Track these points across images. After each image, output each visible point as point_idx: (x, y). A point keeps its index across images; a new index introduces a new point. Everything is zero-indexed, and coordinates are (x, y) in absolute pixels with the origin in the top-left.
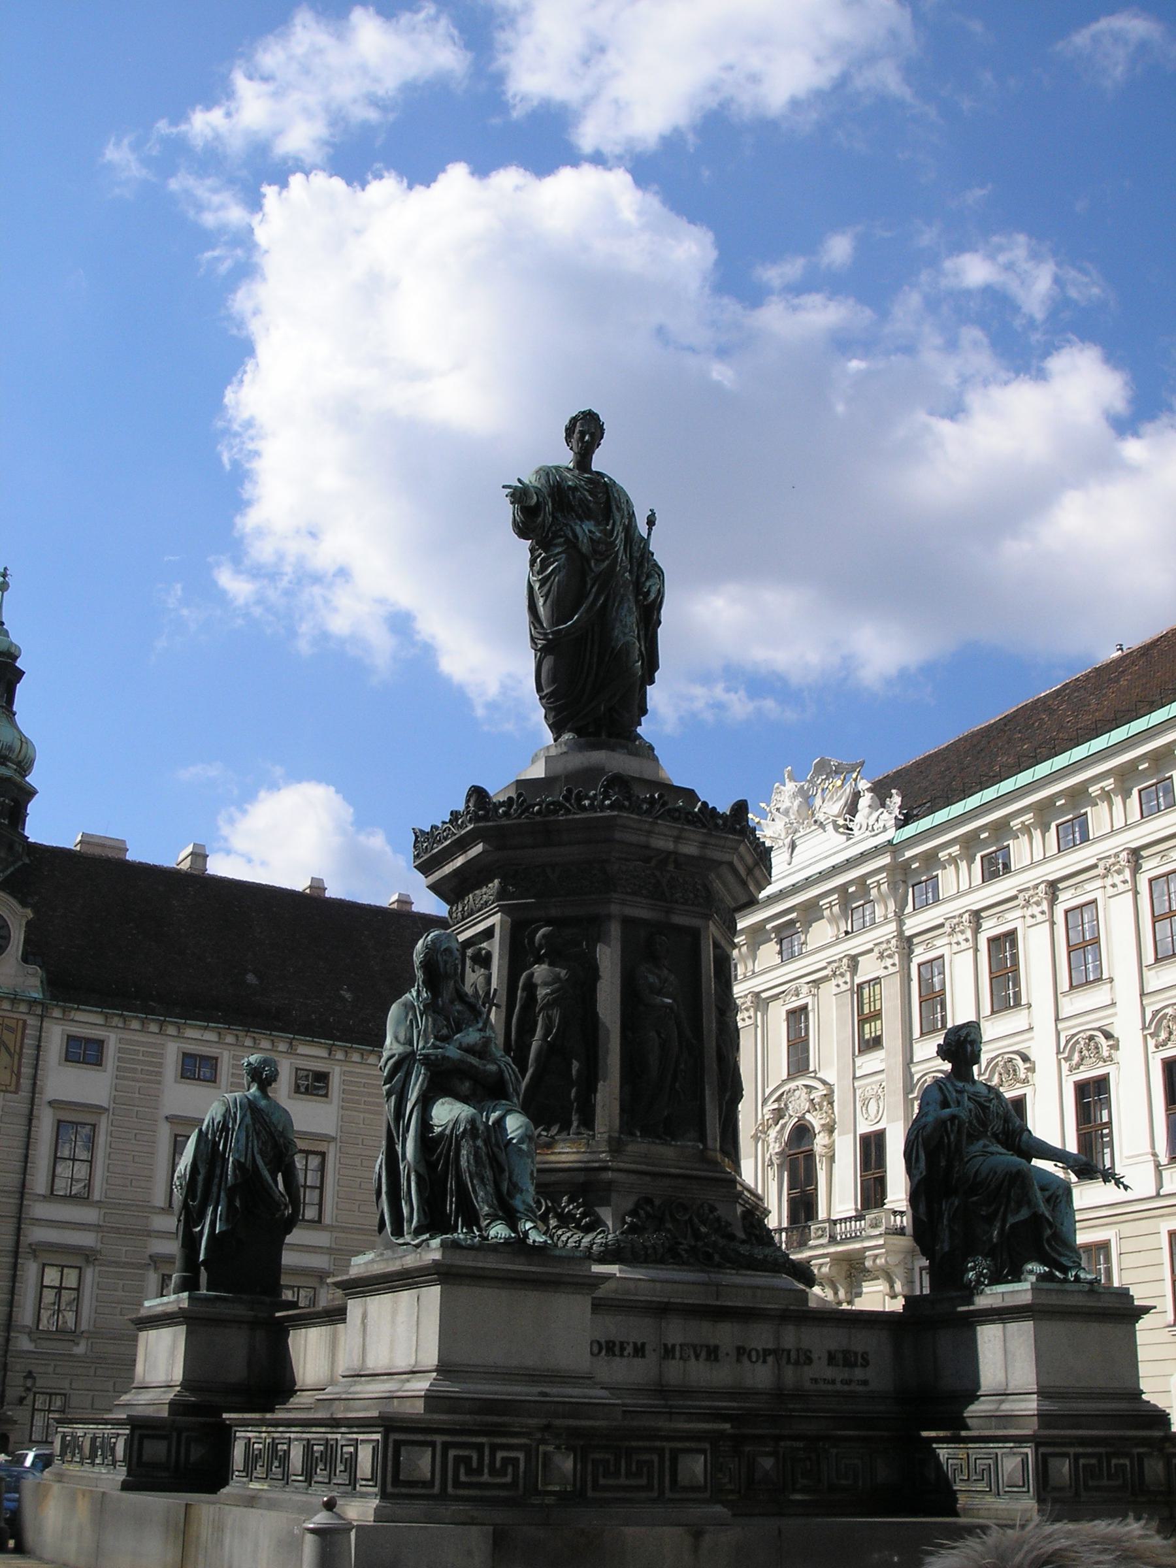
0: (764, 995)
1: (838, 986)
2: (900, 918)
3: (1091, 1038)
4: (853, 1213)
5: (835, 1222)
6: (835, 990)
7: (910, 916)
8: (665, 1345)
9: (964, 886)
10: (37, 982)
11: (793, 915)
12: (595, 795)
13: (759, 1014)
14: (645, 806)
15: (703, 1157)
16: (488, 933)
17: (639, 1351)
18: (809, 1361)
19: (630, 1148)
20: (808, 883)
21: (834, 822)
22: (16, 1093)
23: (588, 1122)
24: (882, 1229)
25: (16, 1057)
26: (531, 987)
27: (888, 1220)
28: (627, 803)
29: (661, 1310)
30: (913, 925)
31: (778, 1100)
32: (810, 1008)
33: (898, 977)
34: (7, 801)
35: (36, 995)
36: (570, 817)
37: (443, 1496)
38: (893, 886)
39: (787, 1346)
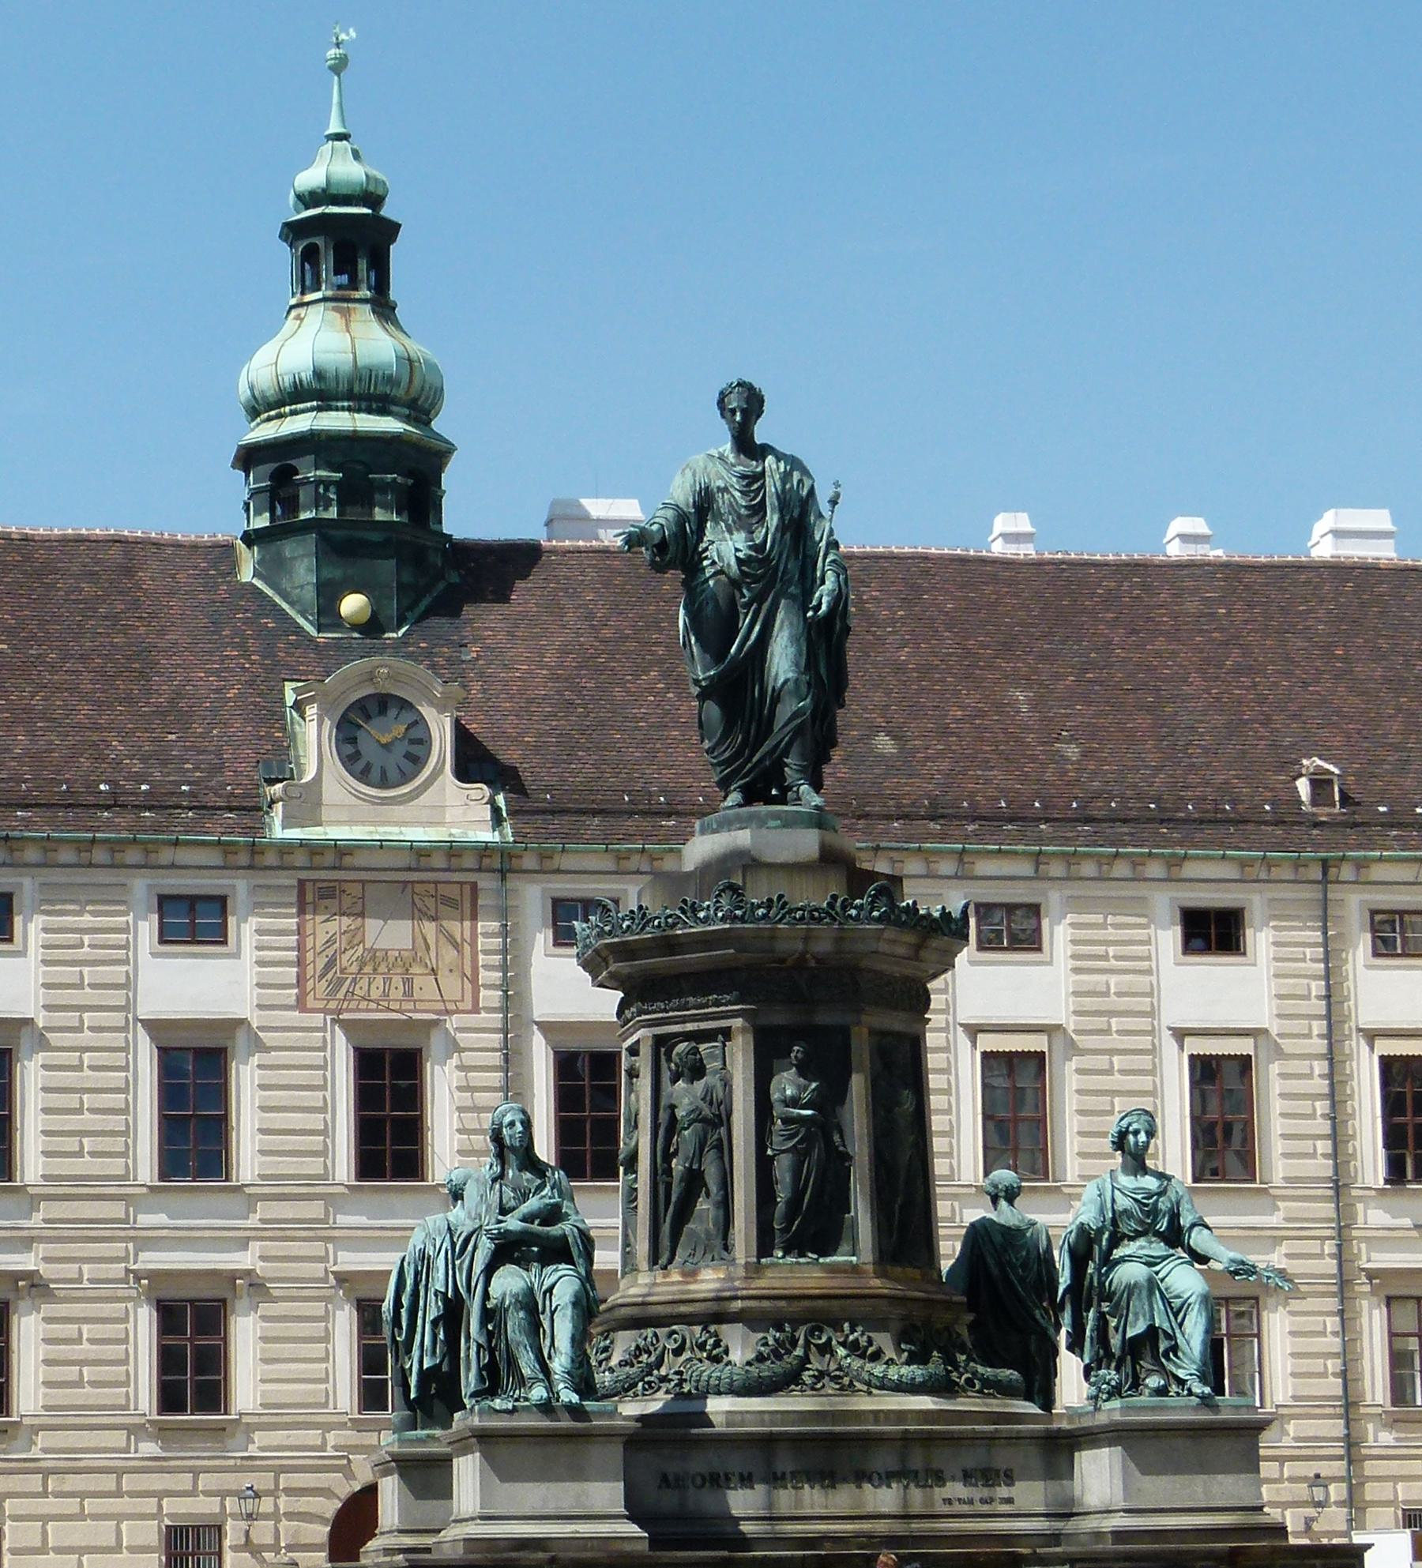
8: (775, 1474)
10: (486, 812)
12: (709, 906)
14: (761, 912)
15: (855, 1269)
18: (940, 1479)
19: (769, 1273)
22: (476, 1009)
23: (726, 1248)
25: (467, 948)
26: (672, 1107)
28: (738, 912)
34: (400, 480)
35: (487, 835)
36: (686, 931)
39: (914, 1467)
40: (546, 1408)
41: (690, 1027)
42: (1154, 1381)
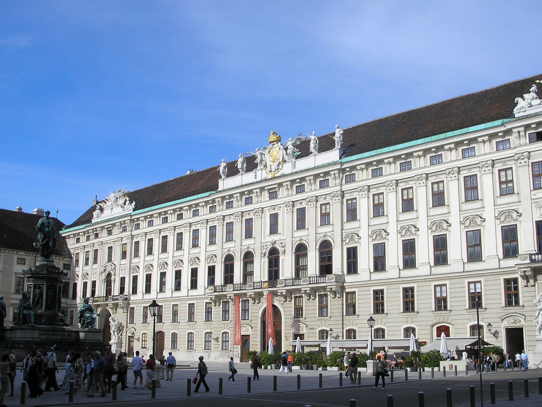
0: (103, 242)
3: (163, 264)
4: (118, 295)
5: (113, 296)
6: (118, 244)
7: (134, 231)
9: (144, 227)
11: (110, 226)
16: (31, 284)
17: (45, 335)
18: (65, 336)
20: (113, 219)
21: (121, 206)
23: (42, 309)
24: (122, 299)
26: (36, 292)
27: (124, 297)
29: (48, 330)
30: (134, 233)
31: (105, 267)
37: (23, 349)
40: (30, 326)
41: (39, 283)
42: (90, 327)
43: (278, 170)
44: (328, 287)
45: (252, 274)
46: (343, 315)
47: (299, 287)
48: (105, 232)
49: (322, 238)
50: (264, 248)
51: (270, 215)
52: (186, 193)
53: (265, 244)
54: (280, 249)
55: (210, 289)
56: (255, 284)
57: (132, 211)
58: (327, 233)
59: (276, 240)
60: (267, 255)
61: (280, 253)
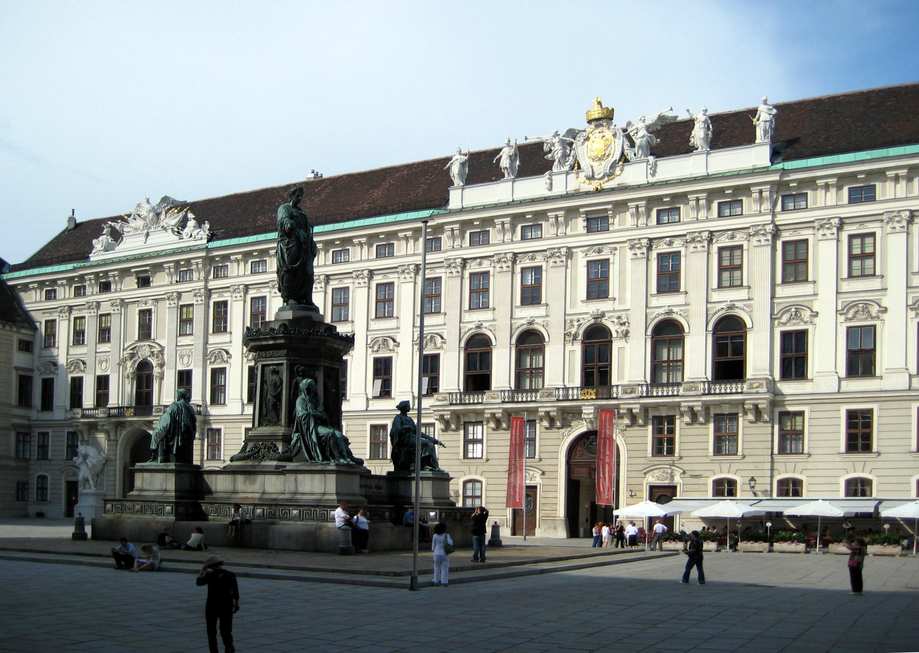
0: (126, 301)
1: (170, 304)
2: (206, 280)
7: (211, 280)
11: (148, 268)
13: (123, 309)
20: (158, 255)
30: (213, 284)
32: (153, 311)
33: (203, 307)
38: (204, 265)
43: (609, 176)
44: (747, 402)
45: (539, 372)
46: (772, 454)
47: (677, 399)
48: (131, 282)
49: (723, 311)
50: (573, 326)
51: (588, 262)
52: (342, 215)
53: (575, 318)
54: (613, 328)
55: (440, 398)
56: (570, 392)
57: (206, 240)
58: (736, 303)
59: (604, 310)
60: (580, 337)
61: (614, 334)
